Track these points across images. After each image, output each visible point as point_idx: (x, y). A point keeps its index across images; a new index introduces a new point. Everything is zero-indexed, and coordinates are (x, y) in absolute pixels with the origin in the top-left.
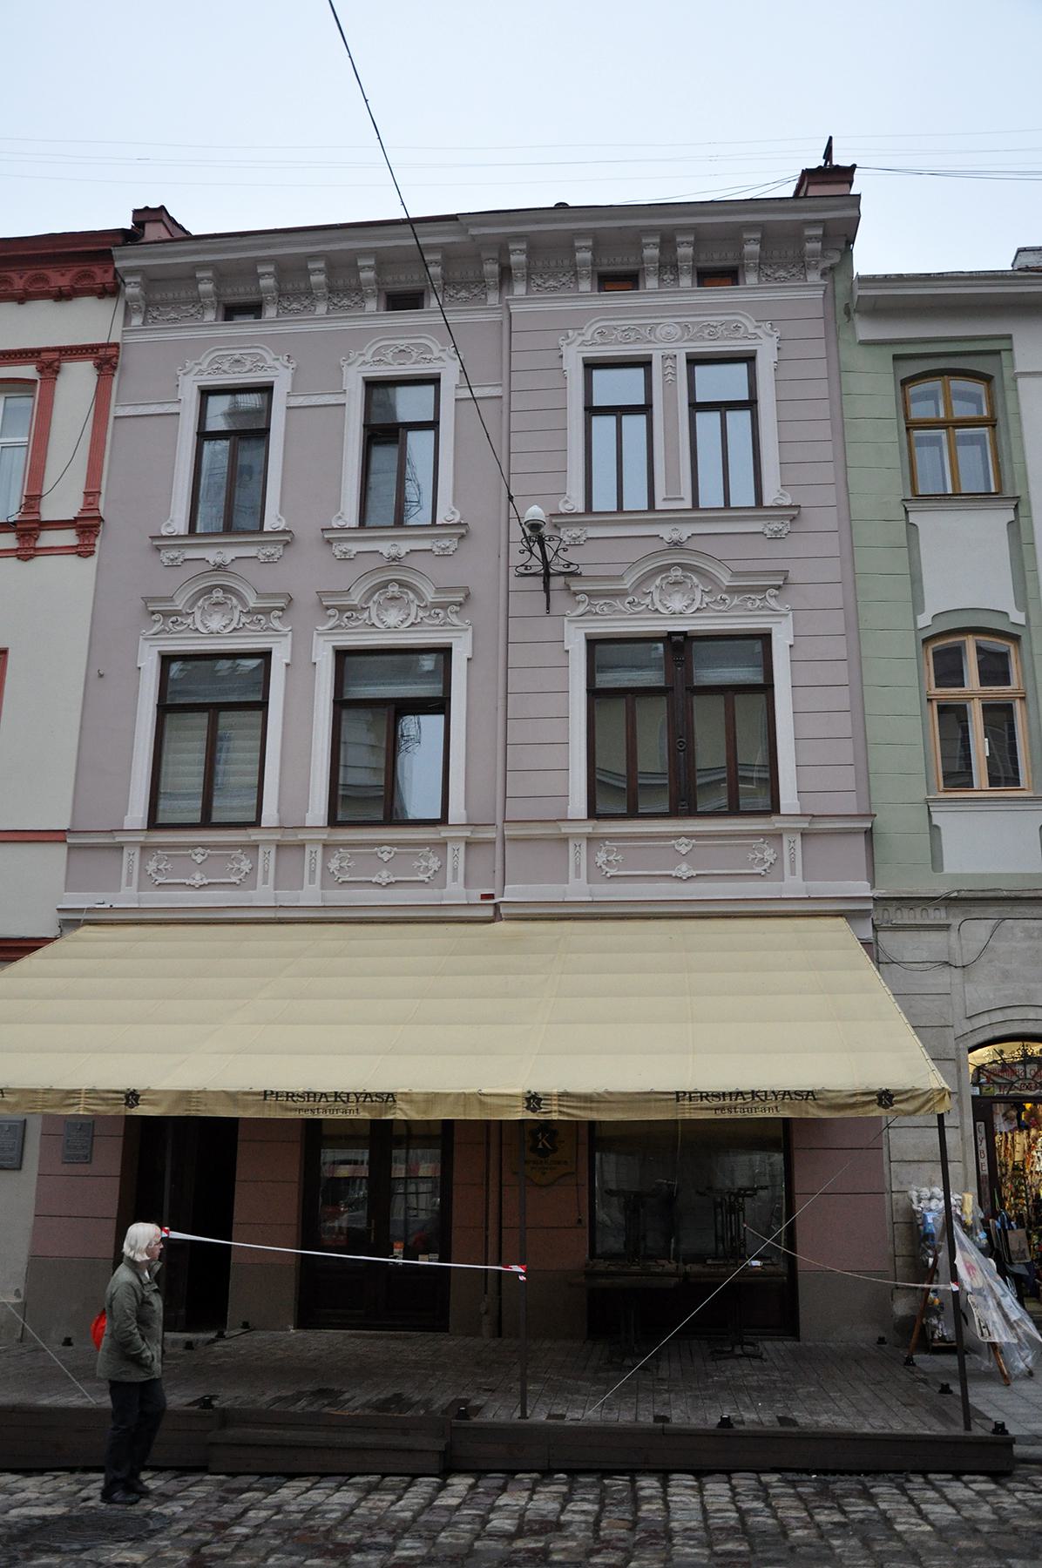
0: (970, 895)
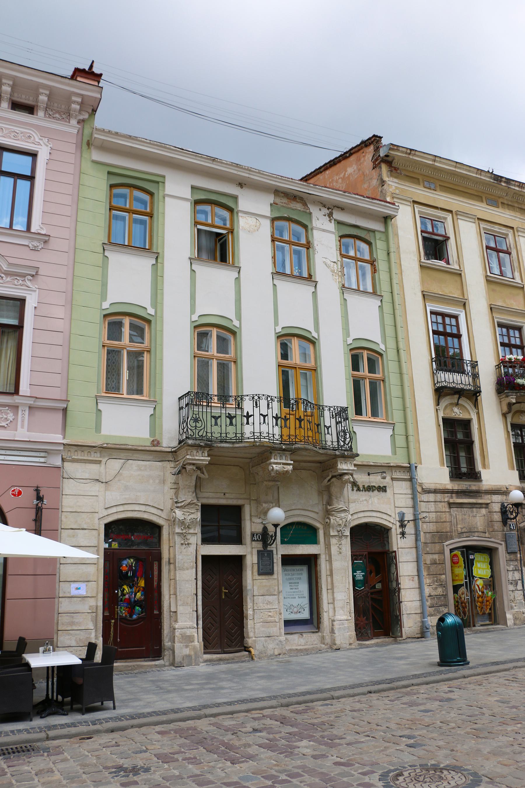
0: (113, 446)
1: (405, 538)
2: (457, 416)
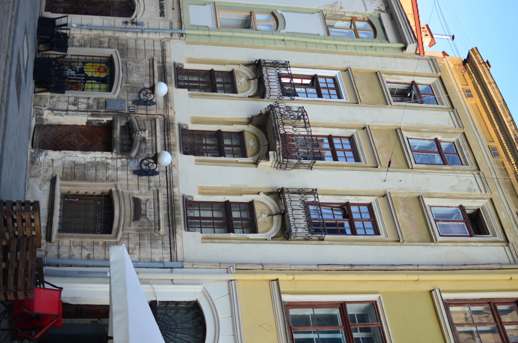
1: (123, 24)
2: (237, 81)
